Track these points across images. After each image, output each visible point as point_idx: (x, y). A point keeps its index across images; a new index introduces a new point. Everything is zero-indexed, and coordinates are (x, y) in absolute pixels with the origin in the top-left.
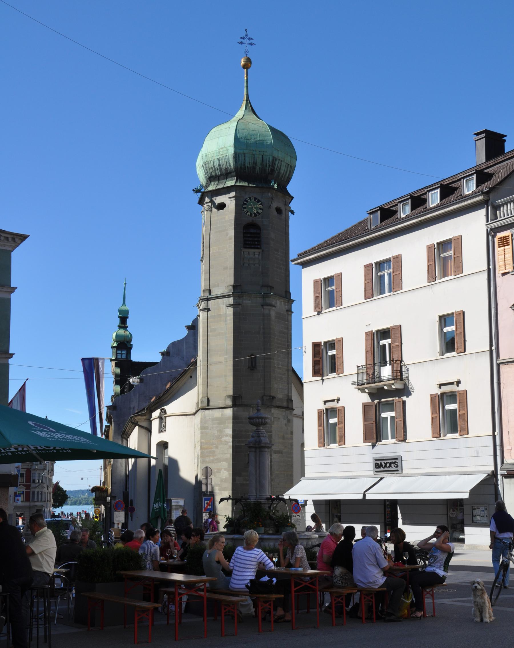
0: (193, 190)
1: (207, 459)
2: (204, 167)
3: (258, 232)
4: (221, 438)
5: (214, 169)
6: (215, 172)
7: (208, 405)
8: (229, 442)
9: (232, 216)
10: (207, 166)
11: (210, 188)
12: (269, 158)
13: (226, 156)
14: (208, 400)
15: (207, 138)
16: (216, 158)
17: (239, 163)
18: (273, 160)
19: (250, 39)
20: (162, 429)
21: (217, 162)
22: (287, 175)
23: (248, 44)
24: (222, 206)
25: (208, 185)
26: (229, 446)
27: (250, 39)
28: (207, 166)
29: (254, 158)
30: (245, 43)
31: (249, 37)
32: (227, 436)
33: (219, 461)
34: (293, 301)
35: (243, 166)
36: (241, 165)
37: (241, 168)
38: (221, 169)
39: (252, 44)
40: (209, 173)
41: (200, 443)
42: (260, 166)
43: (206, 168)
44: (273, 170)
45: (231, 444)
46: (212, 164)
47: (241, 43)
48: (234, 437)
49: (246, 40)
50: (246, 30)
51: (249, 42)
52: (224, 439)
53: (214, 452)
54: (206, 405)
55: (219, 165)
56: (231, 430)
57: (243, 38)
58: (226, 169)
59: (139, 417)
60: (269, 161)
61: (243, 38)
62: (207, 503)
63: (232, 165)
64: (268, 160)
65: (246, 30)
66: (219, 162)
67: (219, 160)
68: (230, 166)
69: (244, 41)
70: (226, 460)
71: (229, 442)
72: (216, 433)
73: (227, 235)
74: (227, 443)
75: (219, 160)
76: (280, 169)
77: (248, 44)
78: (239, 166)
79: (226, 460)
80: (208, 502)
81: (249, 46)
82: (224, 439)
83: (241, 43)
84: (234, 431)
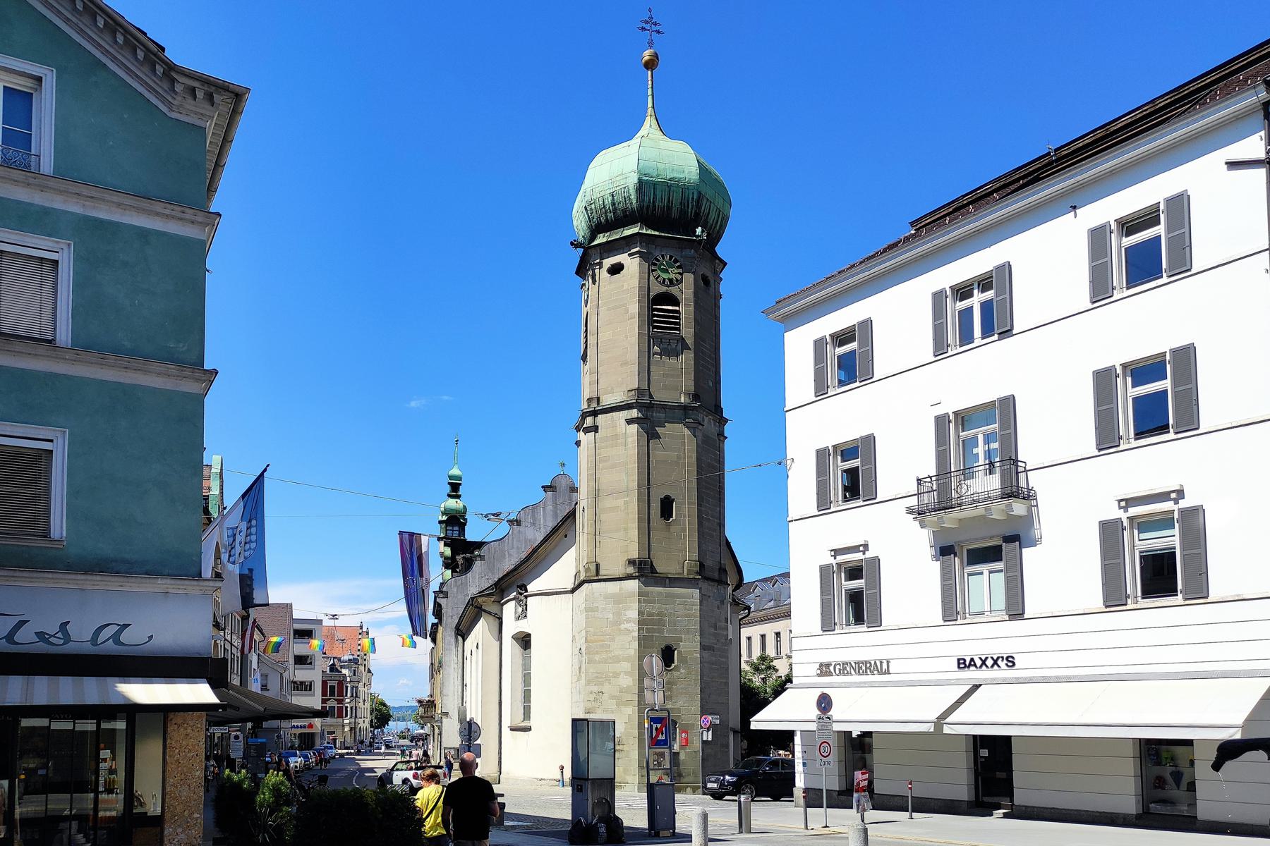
9: (635, 282)
14: (598, 566)
19: (655, 24)
20: (523, 615)
24: (616, 269)
27: (655, 24)
32: (629, 621)
33: (617, 660)
38: (615, 211)
39: (658, 32)
41: (584, 633)
45: (636, 634)
47: (643, 29)
48: (641, 623)
49: (650, 25)
50: (650, 10)
51: (657, 28)
54: (594, 575)
55: (613, 204)
59: (485, 599)
61: (646, 22)
65: (650, 10)
69: (647, 27)
70: (627, 659)
72: (611, 616)
79: (627, 659)
82: (623, 627)
83: (643, 29)
84: (640, 613)
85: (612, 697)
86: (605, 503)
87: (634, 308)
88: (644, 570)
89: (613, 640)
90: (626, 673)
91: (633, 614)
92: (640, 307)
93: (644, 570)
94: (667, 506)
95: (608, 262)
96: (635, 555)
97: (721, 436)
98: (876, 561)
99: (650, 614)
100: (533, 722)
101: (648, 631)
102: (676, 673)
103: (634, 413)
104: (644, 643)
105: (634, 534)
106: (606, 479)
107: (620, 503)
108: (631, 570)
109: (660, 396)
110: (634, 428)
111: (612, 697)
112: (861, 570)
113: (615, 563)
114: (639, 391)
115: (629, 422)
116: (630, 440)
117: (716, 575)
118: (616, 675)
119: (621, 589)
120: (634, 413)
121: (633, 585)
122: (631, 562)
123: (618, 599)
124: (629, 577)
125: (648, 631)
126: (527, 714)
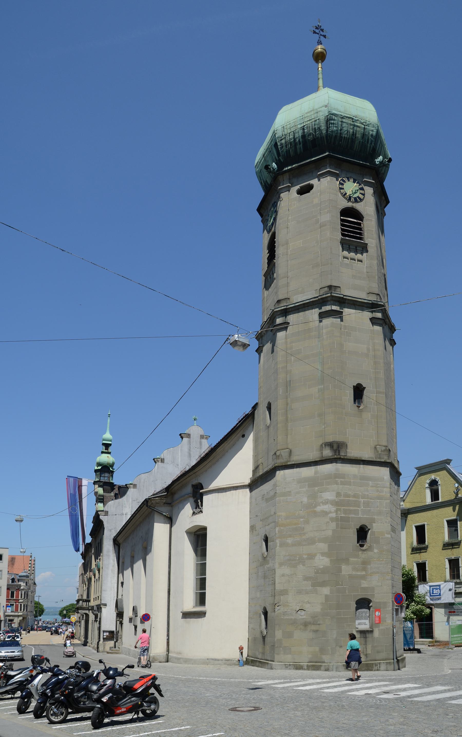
1: (289, 541)
4: (315, 507)
33: (312, 541)
72: (305, 500)
74: (325, 513)
82: (319, 509)
85: (306, 578)
99: (347, 496)
100: (209, 607)
102: (369, 553)
111: (306, 578)
118: (311, 557)
126: (201, 599)
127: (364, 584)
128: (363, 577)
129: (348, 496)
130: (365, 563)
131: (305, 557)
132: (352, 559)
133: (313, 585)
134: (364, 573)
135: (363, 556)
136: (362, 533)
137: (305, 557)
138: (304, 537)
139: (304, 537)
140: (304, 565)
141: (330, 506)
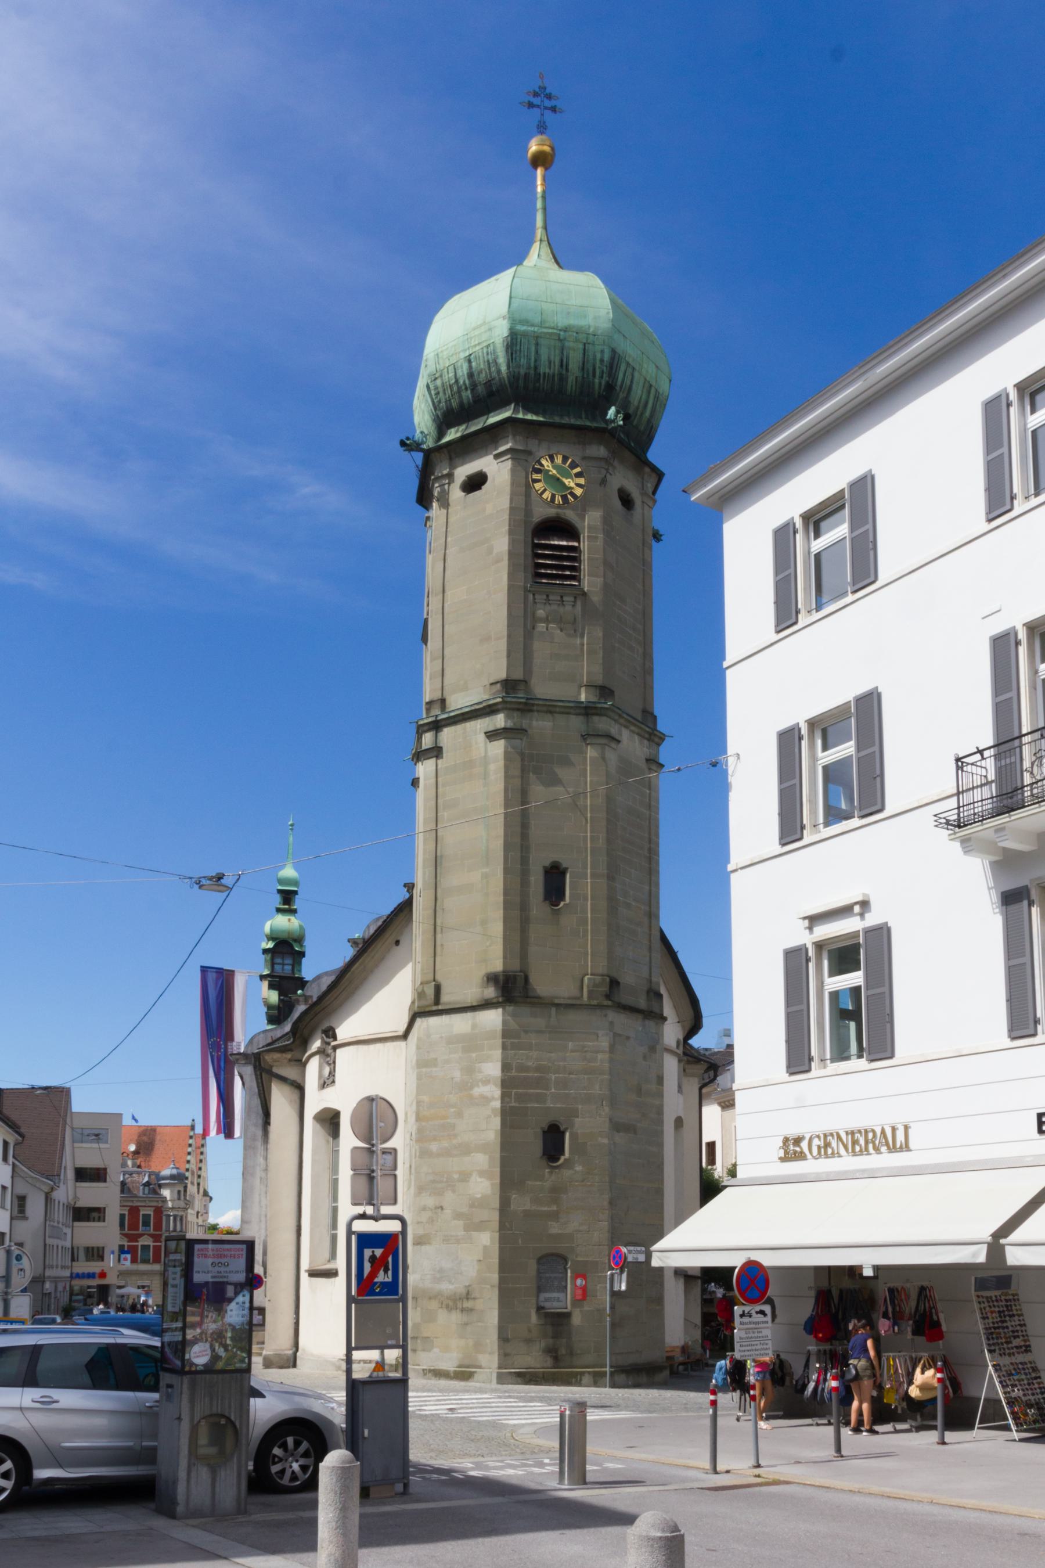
0: (403, 444)
2: (432, 387)
3: (576, 544)
4: (471, 1088)
5: (455, 389)
6: (460, 397)
7: (437, 1000)
8: (493, 1099)
9: (504, 502)
10: (439, 382)
11: (447, 439)
12: (602, 352)
13: (488, 346)
15: (438, 318)
16: (463, 355)
17: (523, 361)
18: (612, 358)
19: (549, 97)
21: (465, 366)
22: (648, 413)
23: (546, 108)
24: (475, 483)
25: (441, 434)
26: (493, 1110)
28: (439, 382)
29: (562, 349)
30: (538, 106)
31: (548, 91)
32: (486, 1082)
33: (466, 1150)
34: (662, 738)
35: (532, 372)
36: (529, 368)
37: (526, 375)
38: (474, 386)
39: (554, 109)
40: (443, 405)
42: (579, 374)
43: (436, 388)
44: (610, 387)
45: (497, 1104)
46: (451, 375)
48: (507, 1084)
50: (542, 77)
52: (478, 1091)
53: (453, 1126)
55: (471, 375)
56: (499, 1065)
57: (536, 95)
58: (488, 383)
60: (602, 361)
61: (536, 95)
62: (373, 1258)
63: (504, 368)
64: (598, 356)
66: (470, 367)
67: (470, 361)
68: (499, 371)
69: (536, 101)
70: (483, 1148)
71: (493, 1099)
72: (457, 1075)
73: (490, 551)
74: (486, 1100)
75: (470, 361)
76: (630, 388)
77: (546, 108)
78: (522, 371)
79: (483, 1148)
80: (378, 1252)
81: (547, 113)
82: (478, 1091)
84: (505, 1067)
85: (458, 1216)
86: (451, 880)
87: (501, 544)
88: (510, 988)
89: (459, 1115)
90: (482, 1173)
91: (493, 1069)
92: (512, 542)
93: (510, 988)
94: (555, 879)
95: (463, 471)
96: (497, 965)
97: (654, 763)
98: (881, 935)
99: (522, 1068)
101: (519, 1098)
103: (499, 720)
104: (511, 1117)
105: (497, 928)
106: (452, 837)
107: (475, 877)
108: (491, 992)
109: (543, 689)
110: (499, 747)
111: (458, 1216)
112: (856, 947)
113: (465, 983)
114: (509, 685)
115: (492, 735)
116: (492, 767)
117: (642, 1003)
118: (465, 1177)
119: (474, 1026)
120: (499, 720)
121: (493, 1018)
122: (492, 979)
123: (469, 1043)
124: (486, 1005)
125: (519, 1098)
127: (554, 1228)
128: (555, 1216)
129: (526, 1069)
130: (557, 1191)
131: (456, 1176)
132: (530, 1183)
133: (467, 1228)
134: (555, 1208)
135: (550, 1178)
136: (553, 1141)
137: (456, 1176)
138: (455, 1142)
139: (455, 1142)
140: (454, 1191)
141: (494, 1088)
